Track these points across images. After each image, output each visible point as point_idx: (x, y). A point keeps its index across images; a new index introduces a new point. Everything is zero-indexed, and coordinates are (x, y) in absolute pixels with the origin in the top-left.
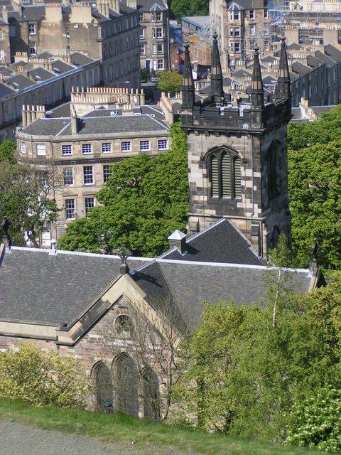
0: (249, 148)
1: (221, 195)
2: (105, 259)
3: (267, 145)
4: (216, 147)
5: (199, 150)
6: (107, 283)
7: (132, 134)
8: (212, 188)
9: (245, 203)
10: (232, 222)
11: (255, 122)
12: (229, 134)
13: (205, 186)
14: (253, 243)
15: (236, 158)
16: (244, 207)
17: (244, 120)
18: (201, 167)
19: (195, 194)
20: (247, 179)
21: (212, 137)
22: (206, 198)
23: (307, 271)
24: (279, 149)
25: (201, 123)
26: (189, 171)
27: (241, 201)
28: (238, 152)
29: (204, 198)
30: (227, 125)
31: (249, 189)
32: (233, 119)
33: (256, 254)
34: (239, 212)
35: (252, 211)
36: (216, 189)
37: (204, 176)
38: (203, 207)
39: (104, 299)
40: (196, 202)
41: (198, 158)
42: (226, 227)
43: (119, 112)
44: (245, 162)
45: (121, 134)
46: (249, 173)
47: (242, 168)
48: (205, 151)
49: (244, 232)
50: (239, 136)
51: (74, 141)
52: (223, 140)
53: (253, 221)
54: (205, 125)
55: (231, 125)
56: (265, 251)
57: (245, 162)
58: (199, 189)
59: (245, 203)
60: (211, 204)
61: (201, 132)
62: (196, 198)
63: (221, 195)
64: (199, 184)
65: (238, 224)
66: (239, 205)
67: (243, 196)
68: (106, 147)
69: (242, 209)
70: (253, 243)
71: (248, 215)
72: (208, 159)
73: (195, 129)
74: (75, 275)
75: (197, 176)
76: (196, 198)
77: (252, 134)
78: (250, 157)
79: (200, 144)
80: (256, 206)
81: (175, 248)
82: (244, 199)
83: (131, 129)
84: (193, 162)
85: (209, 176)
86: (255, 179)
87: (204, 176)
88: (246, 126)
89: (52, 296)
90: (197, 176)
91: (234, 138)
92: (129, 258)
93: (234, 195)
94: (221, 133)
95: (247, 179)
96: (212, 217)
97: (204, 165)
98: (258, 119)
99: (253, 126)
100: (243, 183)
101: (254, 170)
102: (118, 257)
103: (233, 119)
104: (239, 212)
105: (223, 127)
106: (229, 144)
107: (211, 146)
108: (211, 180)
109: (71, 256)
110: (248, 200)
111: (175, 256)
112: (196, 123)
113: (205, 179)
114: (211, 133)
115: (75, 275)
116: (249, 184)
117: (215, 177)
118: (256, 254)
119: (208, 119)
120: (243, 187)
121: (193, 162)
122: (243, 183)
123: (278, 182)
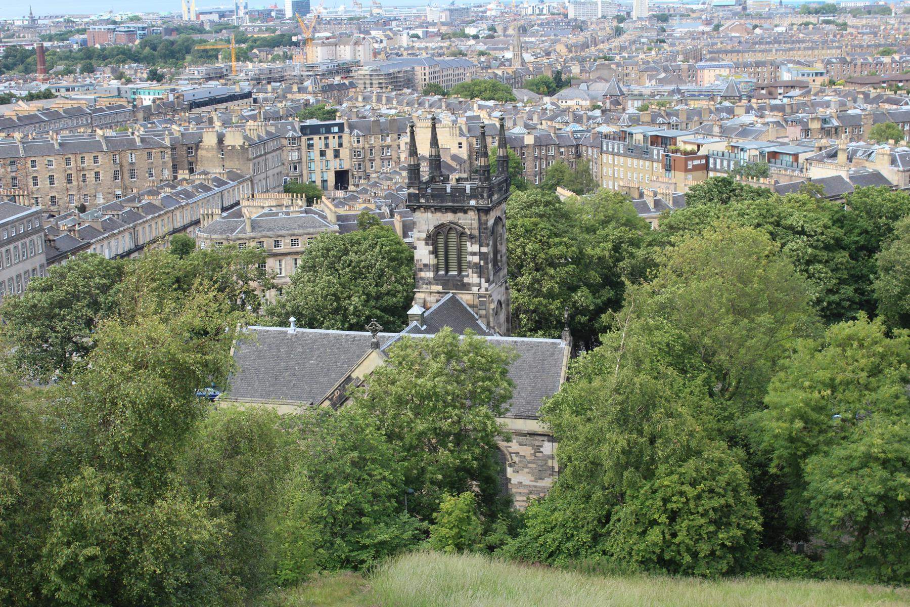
0: (475, 224)
1: (447, 271)
2: (347, 335)
3: (491, 222)
4: (443, 224)
5: (425, 228)
6: (358, 357)
7: (301, 231)
8: (438, 264)
9: (472, 278)
10: (458, 297)
11: (482, 197)
12: (454, 210)
13: (432, 263)
14: (480, 317)
15: (462, 234)
16: (470, 281)
17: (472, 196)
18: (427, 244)
19: (421, 270)
20: (473, 254)
21: (439, 215)
22: (431, 275)
23: (558, 341)
24: (500, 226)
25: (427, 201)
26: (415, 248)
27: (467, 276)
28: (464, 229)
29: (430, 275)
30: (453, 201)
31: (475, 264)
32: (459, 196)
33: (484, 327)
34: (465, 287)
35: (479, 285)
36: (442, 266)
37: (430, 253)
38: (430, 283)
39: (354, 376)
40: (422, 278)
41: (424, 236)
42: (453, 300)
43: (287, 213)
44: (472, 237)
45: (290, 232)
46: (476, 248)
47: (469, 244)
48: (431, 228)
49: (470, 306)
50: (465, 212)
51: (249, 239)
52: (449, 217)
53: (480, 297)
54: (432, 203)
55: (457, 202)
56: (492, 325)
57: (472, 237)
58: (425, 265)
59: (472, 278)
60: (437, 280)
61: (427, 208)
62: (423, 274)
63: (447, 271)
64: (426, 261)
65: (465, 298)
66: (466, 280)
67: (470, 271)
68: (277, 244)
69: (469, 284)
70: (480, 317)
71: (475, 289)
72: (432, 239)
73: (421, 206)
74: (317, 353)
75: (423, 254)
76: (423, 274)
77: (479, 210)
78: (476, 233)
79: (427, 220)
80: (483, 280)
81: (415, 323)
82: (471, 274)
83: (300, 227)
84: (419, 239)
85: (435, 252)
86: (481, 254)
87: (430, 253)
88: (473, 202)
89: (294, 375)
90: (423, 254)
91: (460, 215)
92: (380, 334)
93: (460, 270)
94: (447, 209)
95: (473, 254)
96: (439, 293)
97: (430, 242)
98: (485, 195)
99: (480, 202)
100: (469, 258)
101: (481, 246)
102: (369, 334)
103: (459, 196)
104: (465, 287)
105: (450, 204)
106: (456, 221)
107: (437, 224)
108: (436, 257)
109: (310, 333)
110: (475, 275)
111: (416, 330)
112: (422, 200)
113: (432, 256)
114: (438, 209)
115: (317, 353)
116: (476, 259)
117: (441, 253)
118: (484, 327)
119: (434, 196)
120: (470, 262)
121: (419, 239)
122: (469, 258)
123: (499, 258)
